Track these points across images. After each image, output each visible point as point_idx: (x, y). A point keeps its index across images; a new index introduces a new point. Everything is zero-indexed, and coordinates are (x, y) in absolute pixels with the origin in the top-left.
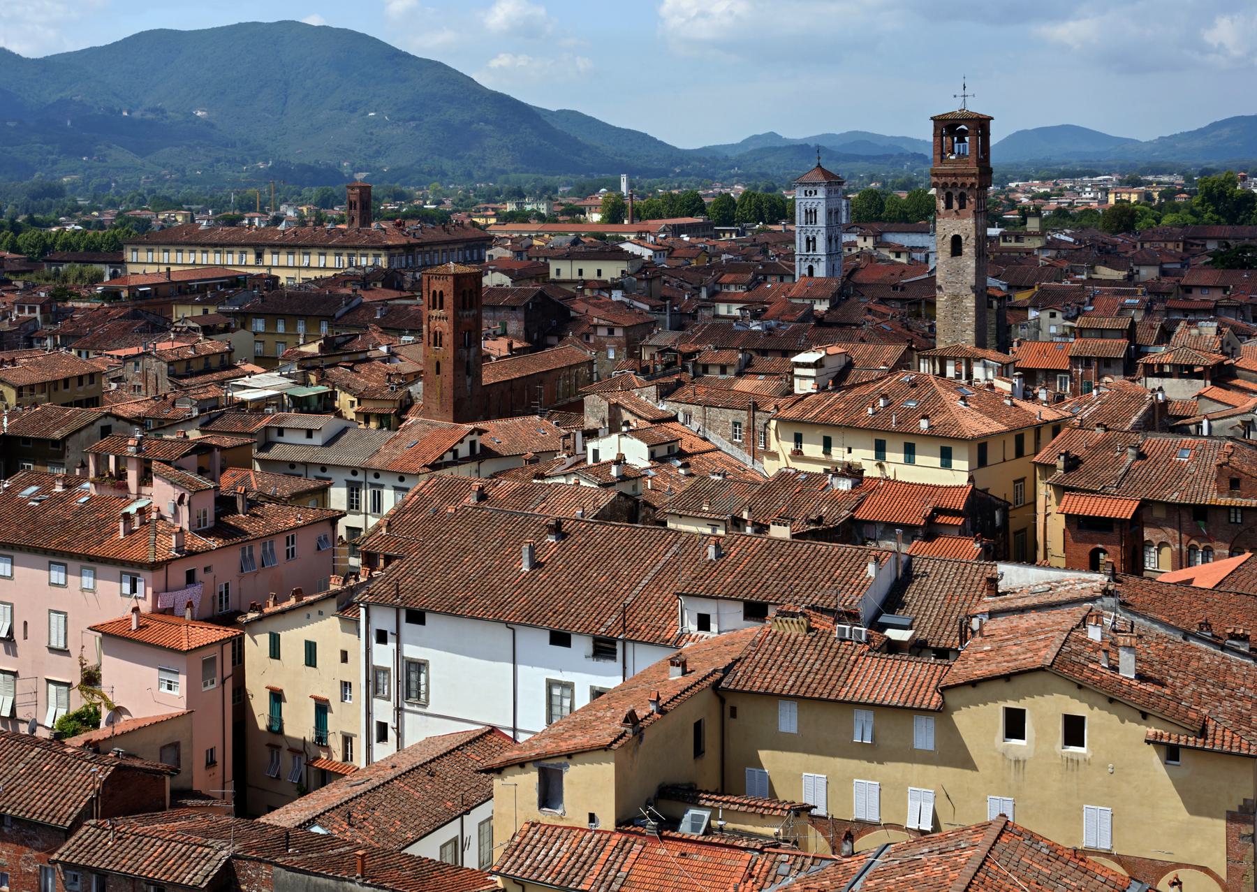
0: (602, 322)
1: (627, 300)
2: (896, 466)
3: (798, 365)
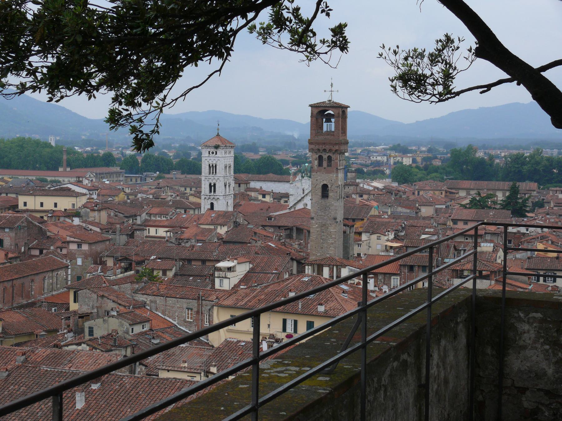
0: (72, 239)
1: (84, 225)
3: (220, 269)
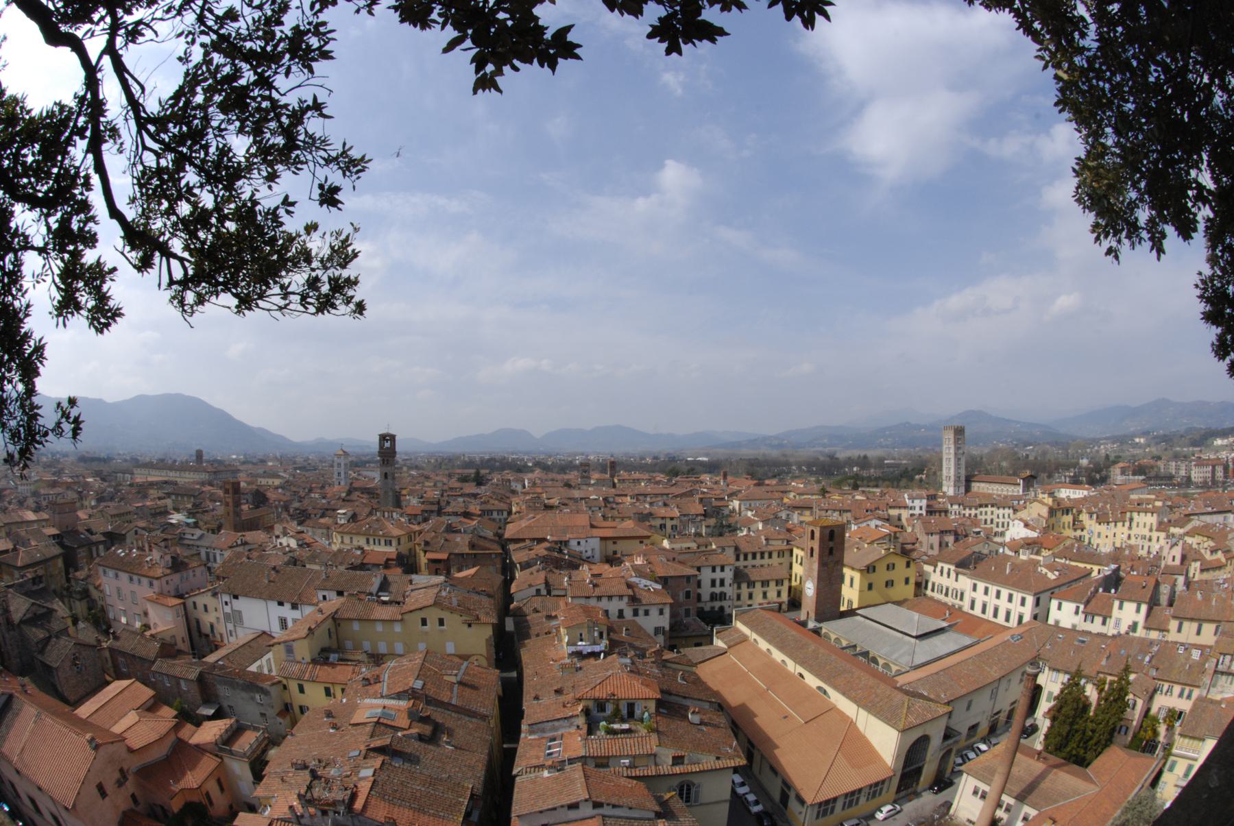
2: (377, 548)
